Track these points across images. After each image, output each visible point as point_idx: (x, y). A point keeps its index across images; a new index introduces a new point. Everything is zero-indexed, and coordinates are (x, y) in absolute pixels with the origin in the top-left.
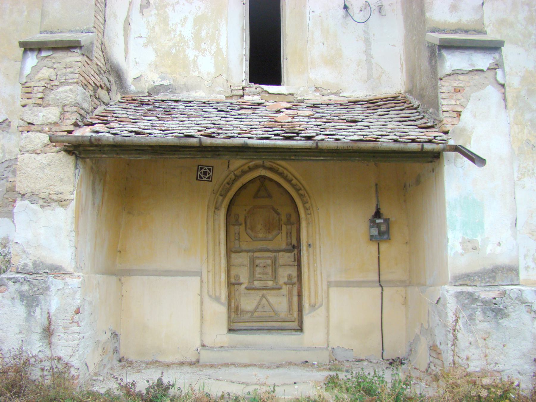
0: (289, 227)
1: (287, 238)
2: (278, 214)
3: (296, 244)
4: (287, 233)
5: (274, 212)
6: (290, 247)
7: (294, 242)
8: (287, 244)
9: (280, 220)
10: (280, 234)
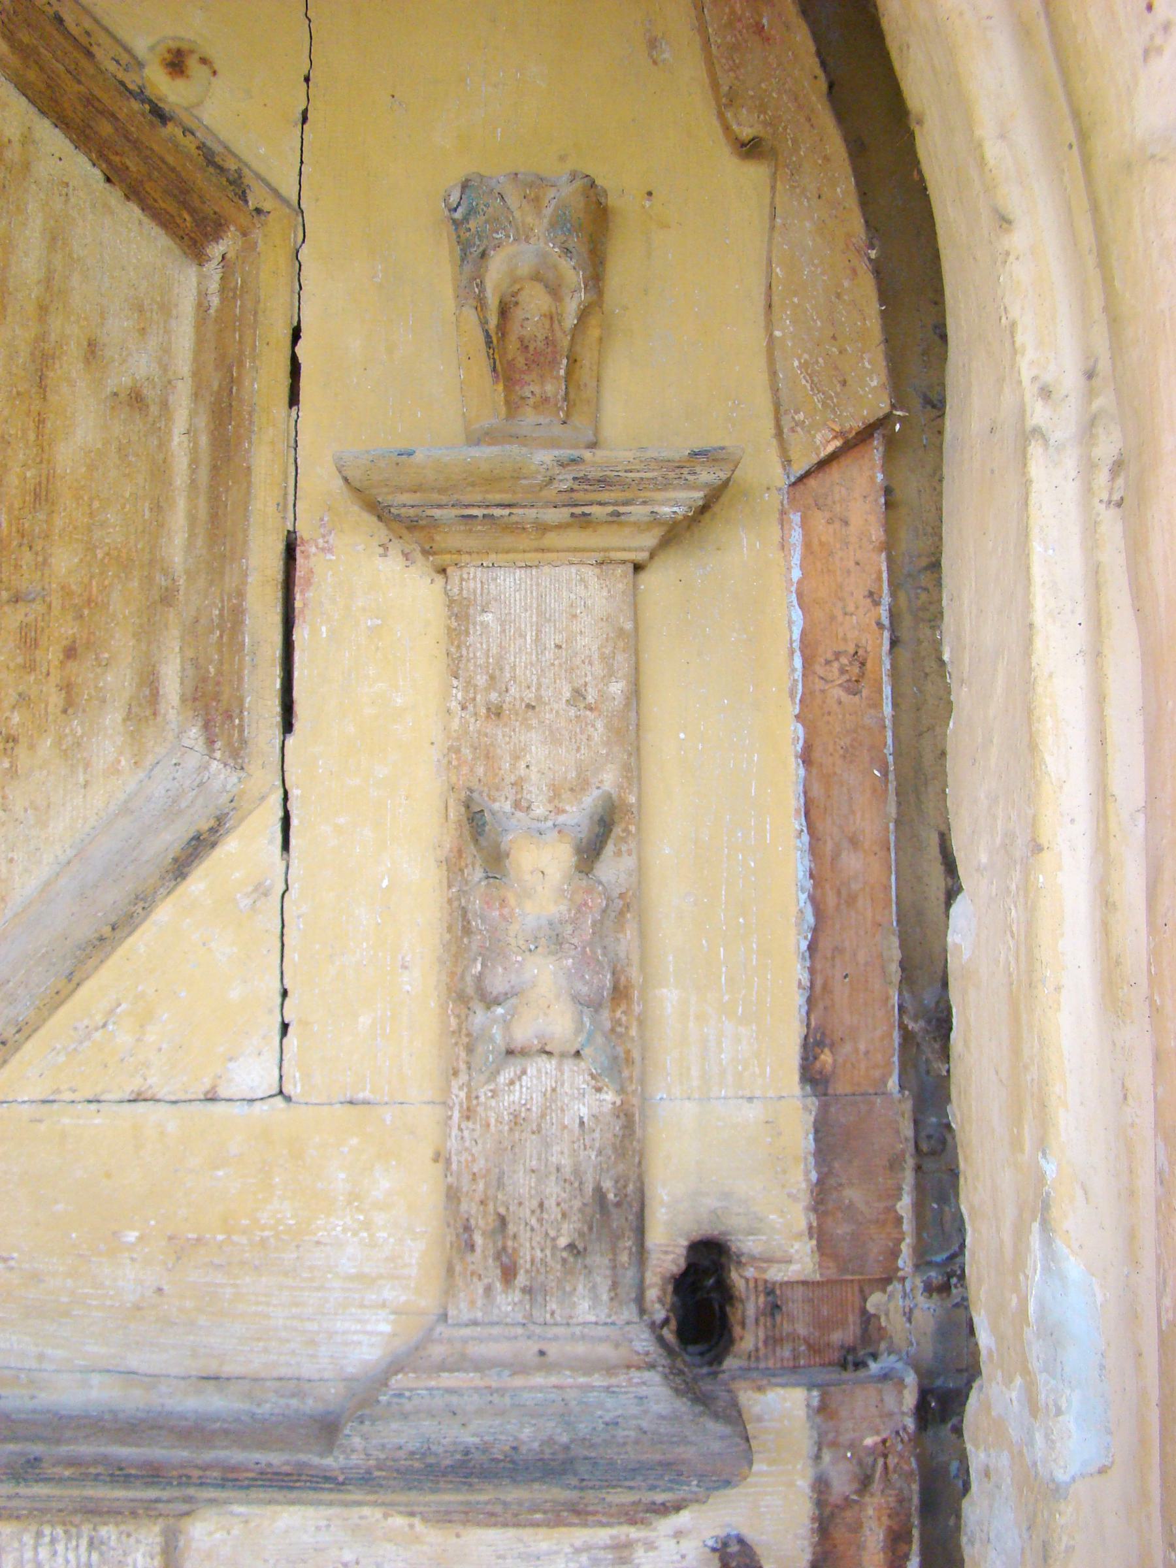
0: (549, 604)
1: (471, 991)
2: (191, 196)
3: (779, 1240)
4: (479, 836)
5: (57, 155)
6: (593, 1344)
7: (733, 1147)
8: (478, 1237)
9: (247, 376)
10: (249, 846)
